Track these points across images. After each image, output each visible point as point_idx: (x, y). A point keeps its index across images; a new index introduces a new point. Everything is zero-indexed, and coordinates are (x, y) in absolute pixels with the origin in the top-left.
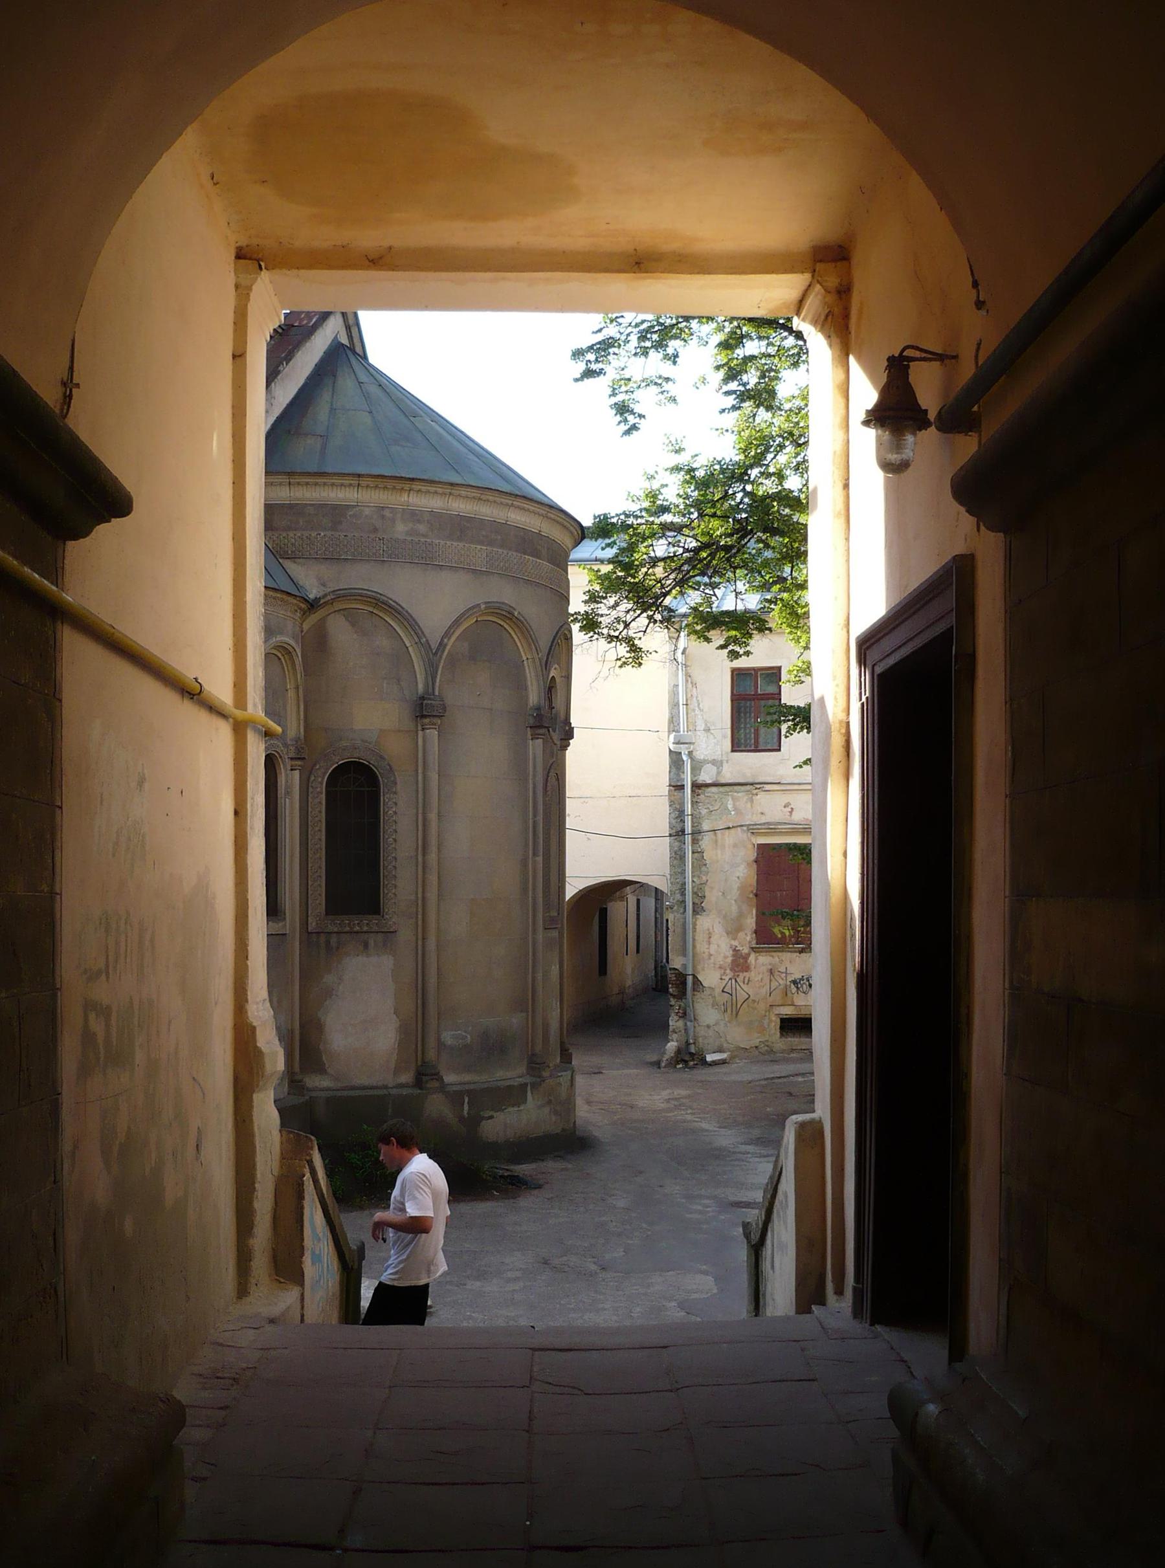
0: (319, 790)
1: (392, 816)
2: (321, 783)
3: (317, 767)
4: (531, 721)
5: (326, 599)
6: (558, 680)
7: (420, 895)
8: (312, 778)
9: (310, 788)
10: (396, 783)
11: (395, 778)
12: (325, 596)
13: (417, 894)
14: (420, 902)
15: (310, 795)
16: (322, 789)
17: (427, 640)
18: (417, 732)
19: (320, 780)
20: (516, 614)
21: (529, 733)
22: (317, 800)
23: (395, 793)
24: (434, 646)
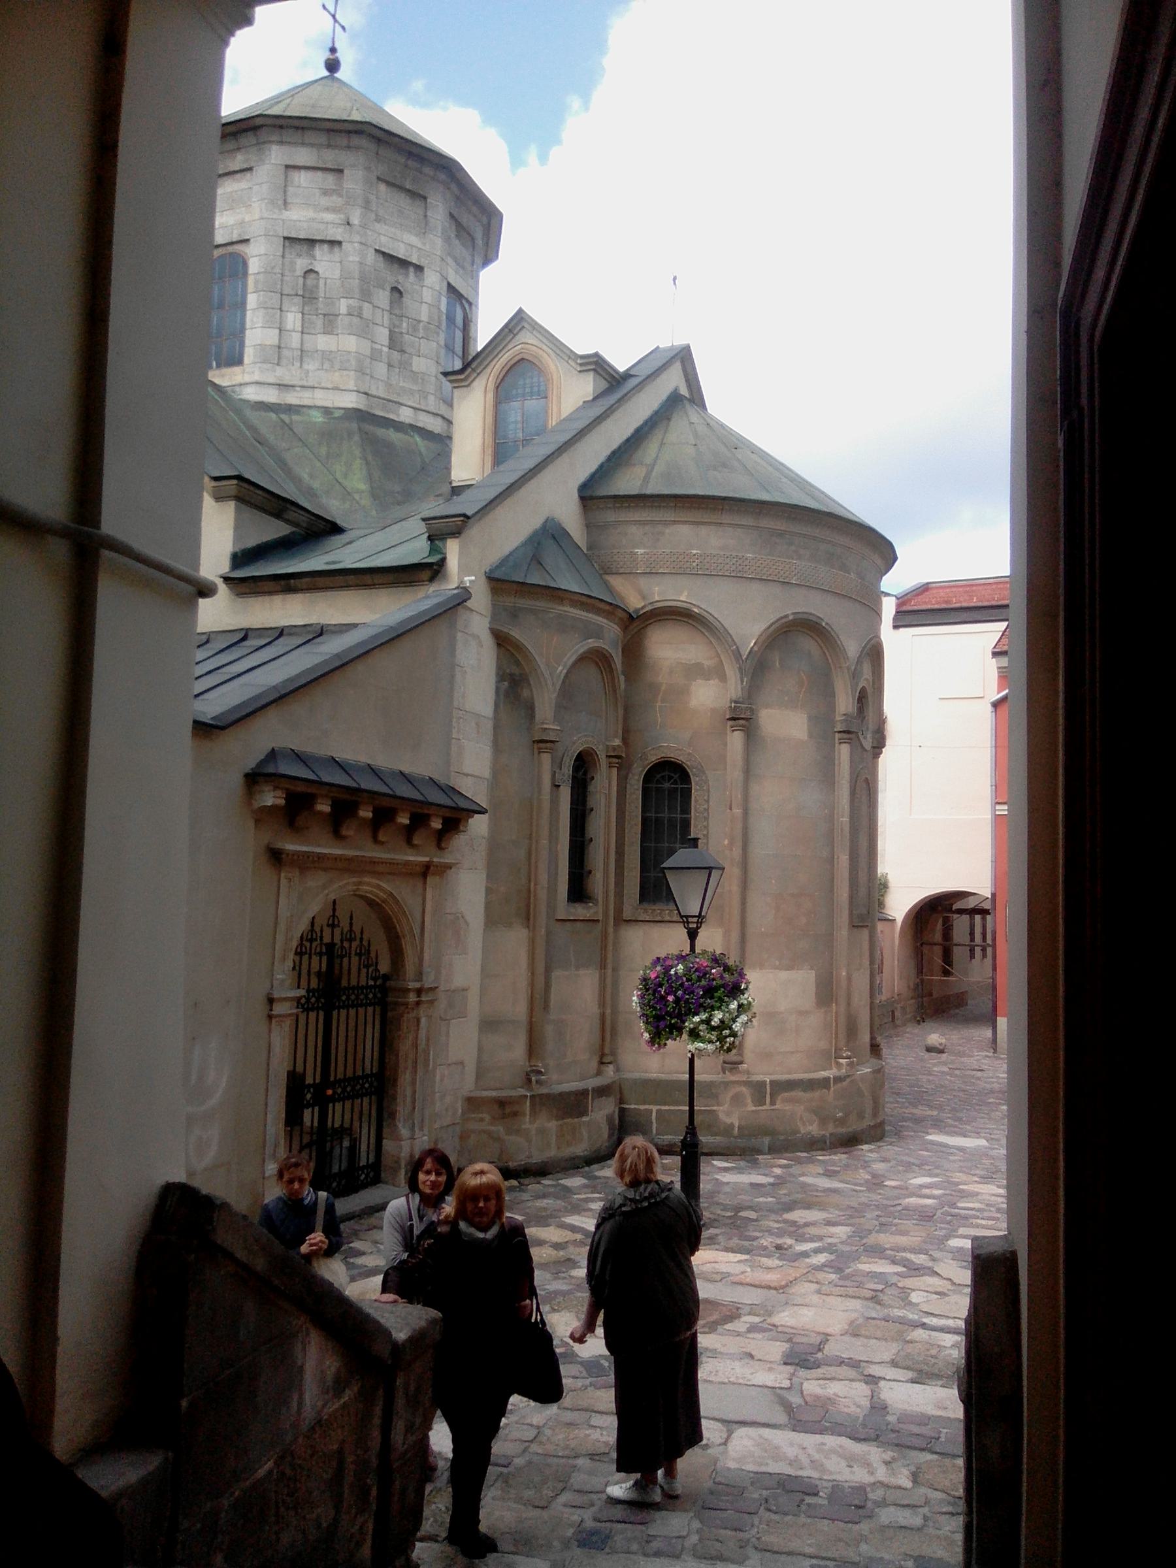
0: (636, 787)
2: (639, 781)
4: (839, 728)
5: (644, 611)
6: (870, 691)
8: (630, 775)
12: (643, 608)
15: (628, 792)
17: (737, 647)
19: (636, 777)
20: (824, 624)
21: (837, 741)
22: (635, 796)
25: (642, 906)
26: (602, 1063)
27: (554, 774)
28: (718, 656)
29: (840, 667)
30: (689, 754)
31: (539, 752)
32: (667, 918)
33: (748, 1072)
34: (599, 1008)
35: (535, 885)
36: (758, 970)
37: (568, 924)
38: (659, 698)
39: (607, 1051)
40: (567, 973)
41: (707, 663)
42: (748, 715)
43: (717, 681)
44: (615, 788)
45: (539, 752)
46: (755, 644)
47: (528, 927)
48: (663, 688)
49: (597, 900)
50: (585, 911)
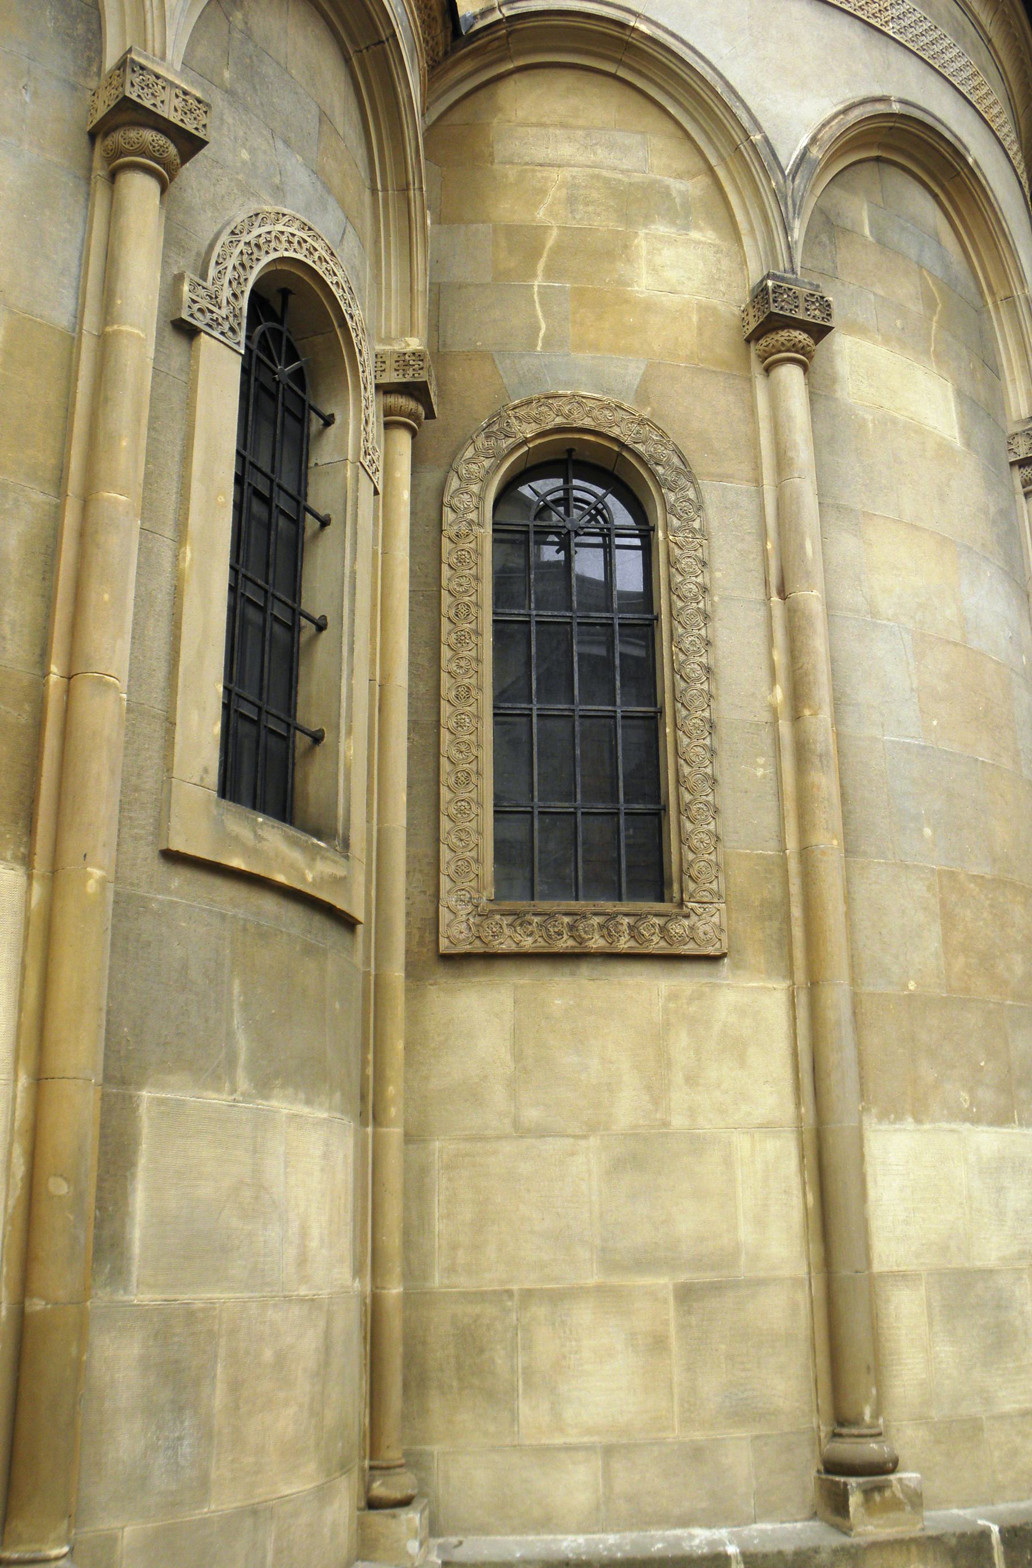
0: (473, 516)
2: (481, 498)
3: (469, 453)
7: (792, 844)
8: (454, 483)
9: (446, 510)
10: (700, 508)
11: (698, 491)
12: (483, 14)
13: (782, 840)
14: (793, 866)
15: (449, 531)
17: (766, 139)
18: (750, 380)
19: (475, 488)
20: (970, 161)
23: (704, 533)
24: (788, 158)
25: (507, 905)
26: (373, 1504)
28: (711, 169)
29: (1009, 299)
30: (642, 422)
32: (596, 943)
33: (916, 1500)
34: (357, 1271)
35: (69, 677)
36: (909, 1122)
37: (225, 891)
39: (393, 1454)
40: (216, 1099)
41: (677, 186)
42: (814, 315)
44: (406, 495)
45: (113, 176)
46: (814, 140)
47: (27, 861)
48: (550, 243)
49: (346, 844)
50: (296, 856)
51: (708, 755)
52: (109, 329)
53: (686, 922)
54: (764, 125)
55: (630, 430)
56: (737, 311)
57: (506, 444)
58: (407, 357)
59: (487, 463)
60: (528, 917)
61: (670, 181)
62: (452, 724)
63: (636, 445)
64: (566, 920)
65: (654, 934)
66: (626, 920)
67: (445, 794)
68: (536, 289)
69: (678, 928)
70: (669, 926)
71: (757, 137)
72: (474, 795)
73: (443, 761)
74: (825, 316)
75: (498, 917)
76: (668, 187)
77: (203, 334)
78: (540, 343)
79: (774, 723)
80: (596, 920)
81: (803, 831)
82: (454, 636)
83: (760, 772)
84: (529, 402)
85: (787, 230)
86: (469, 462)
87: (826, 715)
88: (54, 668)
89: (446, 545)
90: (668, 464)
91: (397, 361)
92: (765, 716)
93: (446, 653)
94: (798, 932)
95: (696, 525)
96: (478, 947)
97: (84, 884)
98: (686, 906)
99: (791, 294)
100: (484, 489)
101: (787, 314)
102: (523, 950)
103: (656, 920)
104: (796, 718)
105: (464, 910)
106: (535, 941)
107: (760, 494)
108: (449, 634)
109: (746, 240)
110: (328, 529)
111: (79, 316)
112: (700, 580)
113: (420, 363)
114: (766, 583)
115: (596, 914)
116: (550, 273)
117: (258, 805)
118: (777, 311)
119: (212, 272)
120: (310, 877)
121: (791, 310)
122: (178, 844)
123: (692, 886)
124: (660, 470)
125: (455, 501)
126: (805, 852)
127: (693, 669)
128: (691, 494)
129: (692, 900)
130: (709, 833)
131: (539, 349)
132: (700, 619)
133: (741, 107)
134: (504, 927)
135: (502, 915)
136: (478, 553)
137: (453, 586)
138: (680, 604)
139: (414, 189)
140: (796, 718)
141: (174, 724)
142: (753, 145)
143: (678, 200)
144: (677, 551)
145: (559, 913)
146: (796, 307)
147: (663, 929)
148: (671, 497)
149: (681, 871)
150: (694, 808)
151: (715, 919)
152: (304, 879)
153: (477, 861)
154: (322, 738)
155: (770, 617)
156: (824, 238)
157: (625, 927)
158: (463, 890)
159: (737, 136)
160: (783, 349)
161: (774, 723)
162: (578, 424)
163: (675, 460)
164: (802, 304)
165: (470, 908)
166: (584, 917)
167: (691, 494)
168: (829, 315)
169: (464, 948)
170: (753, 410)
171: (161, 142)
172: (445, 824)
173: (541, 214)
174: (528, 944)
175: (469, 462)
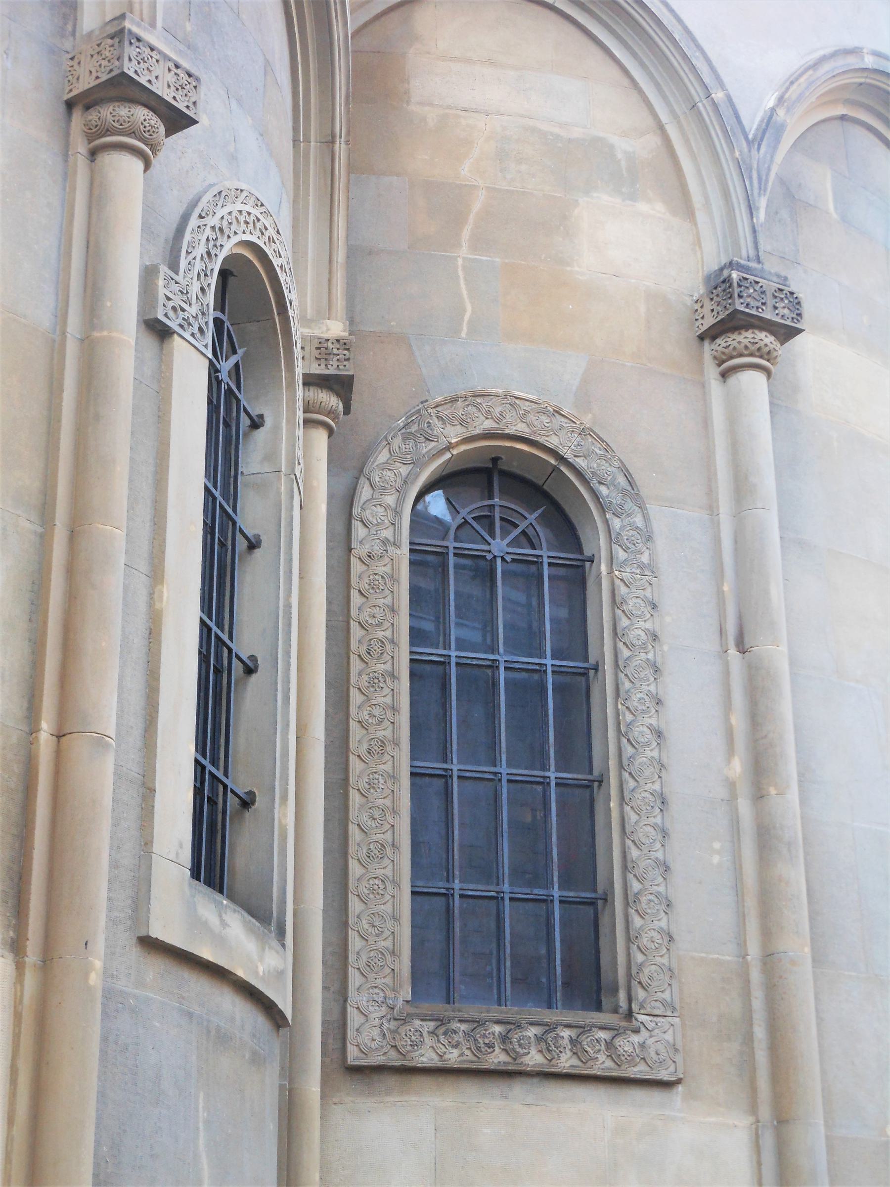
0: (387, 534)
1: (644, 647)
2: (397, 512)
3: (383, 456)
7: (754, 950)
8: (365, 492)
9: (356, 525)
10: (649, 538)
11: (646, 518)
13: (742, 944)
14: (756, 976)
15: (359, 550)
16: (397, 530)
17: (729, 98)
19: (390, 500)
23: (651, 569)
24: (752, 123)
25: (426, 1007)
27: (149, 274)
28: (661, 128)
30: (584, 432)
31: (93, 154)
32: (534, 1059)
38: (466, 233)
41: (622, 145)
43: (659, 208)
45: (93, 154)
46: (781, 100)
48: (477, 206)
49: (281, 933)
51: (660, 837)
52: (96, 334)
53: (636, 1039)
54: (726, 79)
55: (570, 441)
56: (689, 301)
57: (426, 448)
58: (330, 344)
59: (404, 470)
60: (455, 1025)
61: (614, 139)
62: (363, 785)
63: (577, 459)
64: (497, 1029)
65: (599, 1050)
66: (566, 1033)
67: (355, 869)
68: (460, 261)
69: (627, 1044)
70: (618, 1042)
71: (718, 96)
72: (388, 872)
73: (353, 829)
74: (795, 316)
75: (417, 1023)
76: (612, 147)
77: (175, 336)
78: (465, 328)
79: (732, 798)
80: (532, 1032)
81: (767, 934)
82: (365, 678)
83: (716, 859)
84: (454, 400)
85: (751, 210)
86: (386, 466)
87: (793, 794)
88: (44, 725)
89: (357, 567)
90: (613, 484)
91: (318, 348)
92: (722, 792)
93: (356, 698)
94: (762, 1057)
95: (645, 559)
96: (393, 1059)
97: (86, 976)
98: (636, 1019)
99: (757, 288)
100: (400, 502)
101: (754, 312)
102: (448, 1065)
103: (603, 1035)
104: (759, 796)
105: (376, 1013)
106: (462, 1055)
107: (716, 525)
108: (360, 674)
109: (701, 216)
110: (258, 552)
111: (61, 316)
112: (648, 625)
113: (346, 352)
114: (722, 632)
115: (532, 1024)
116: (479, 243)
117: (212, 885)
118: (742, 308)
119: (183, 264)
120: (261, 970)
121: (758, 308)
122: (157, 932)
123: (641, 994)
124: (604, 490)
125: (367, 514)
126: (769, 959)
127: (640, 732)
128: (639, 521)
129: (642, 1011)
130: (660, 931)
131: (463, 335)
132: (648, 672)
133: (702, 58)
134: (425, 1034)
135: (422, 1020)
136: (394, 578)
137: (365, 616)
138: (626, 653)
139: (340, 142)
140: (759, 796)
141: (152, 790)
142: (715, 105)
143: (623, 164)
144: (623, 590)
145: (490, 1021)
146: (764, 304)
147: (609, 1045)
148: (616, 523)
149: (629, 976)
150: (644, 899)
151: (669, 1037)
152: (256, 973)
153: (393, 953)
154: (253, 802)
155: (727, 673)
156: (785, 214)
157: (566, 1042)
158: (376, 987)
159: (696, 92)
160: (746, 352)
161: (732, 798)
162: (511, 430)
163: (621, 480)
164: (770, 302)
165: (384, 1010)
166: (519, 1027)
167: (639, 521)
168: (799, 315)
169: (377, 1059)
170: (706, 422)
171: (153, 123)
172: (355, 907)
173: (466, 170)
174: (453, 1057)
175: (386, 466)
